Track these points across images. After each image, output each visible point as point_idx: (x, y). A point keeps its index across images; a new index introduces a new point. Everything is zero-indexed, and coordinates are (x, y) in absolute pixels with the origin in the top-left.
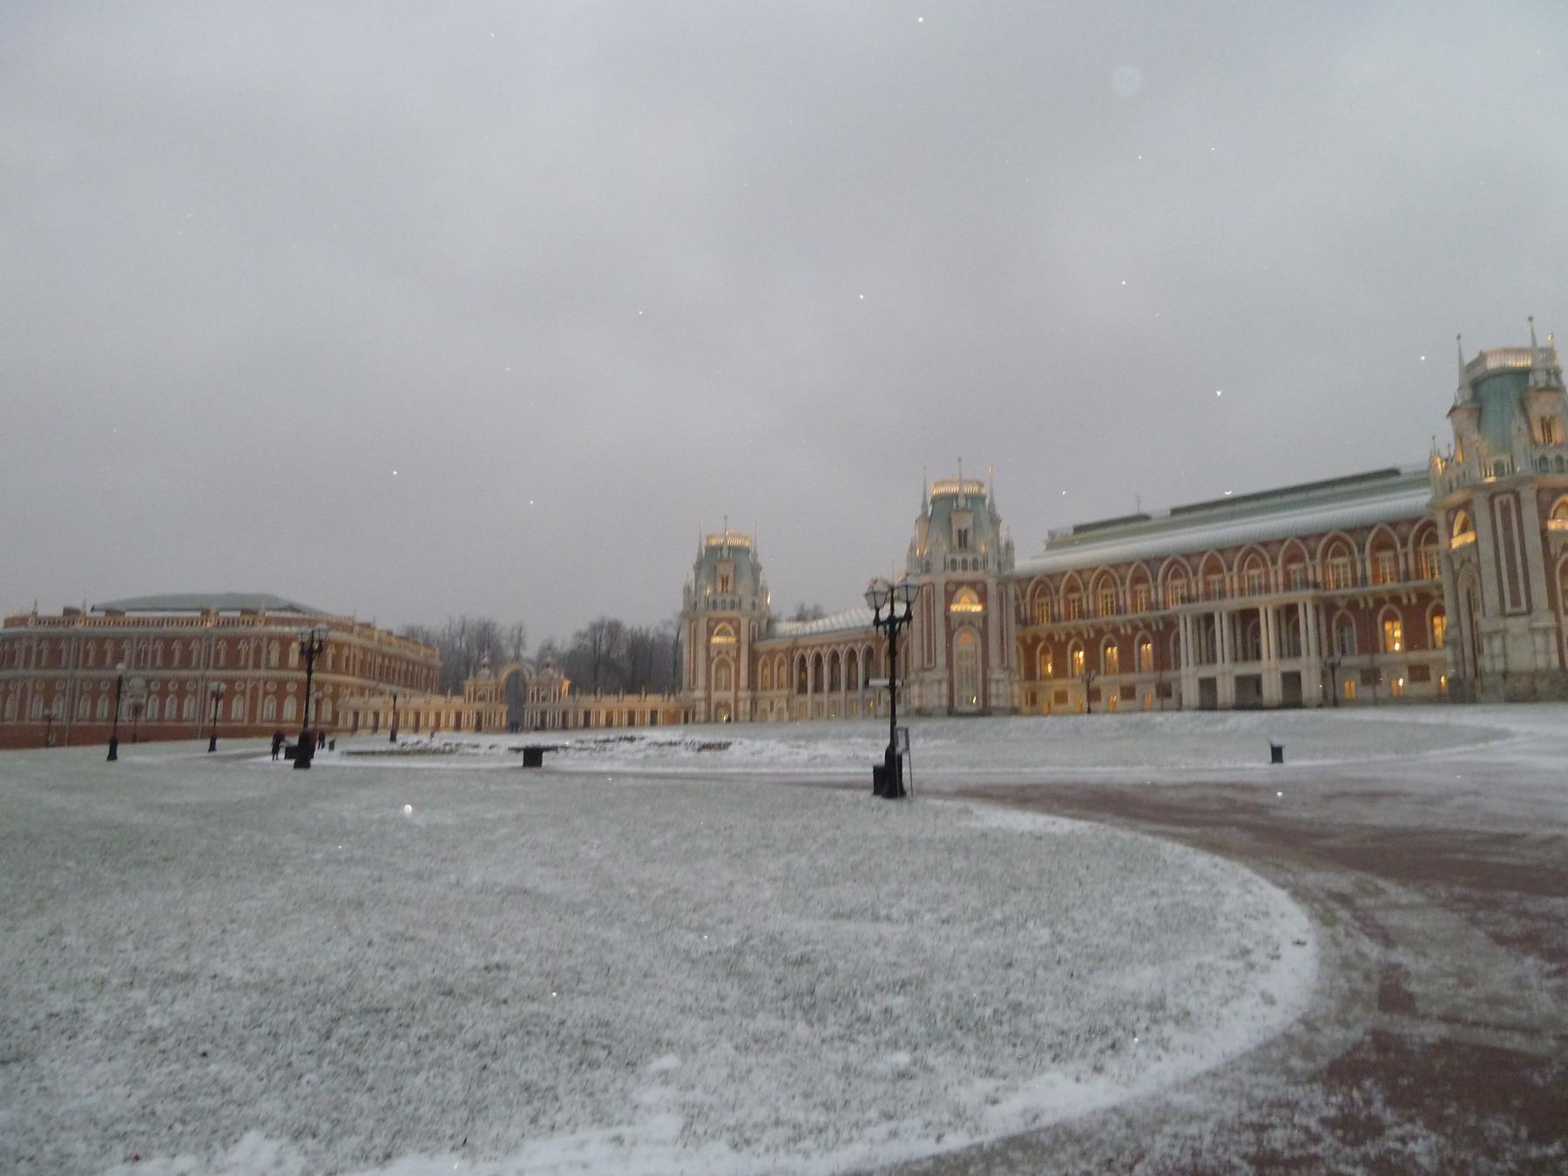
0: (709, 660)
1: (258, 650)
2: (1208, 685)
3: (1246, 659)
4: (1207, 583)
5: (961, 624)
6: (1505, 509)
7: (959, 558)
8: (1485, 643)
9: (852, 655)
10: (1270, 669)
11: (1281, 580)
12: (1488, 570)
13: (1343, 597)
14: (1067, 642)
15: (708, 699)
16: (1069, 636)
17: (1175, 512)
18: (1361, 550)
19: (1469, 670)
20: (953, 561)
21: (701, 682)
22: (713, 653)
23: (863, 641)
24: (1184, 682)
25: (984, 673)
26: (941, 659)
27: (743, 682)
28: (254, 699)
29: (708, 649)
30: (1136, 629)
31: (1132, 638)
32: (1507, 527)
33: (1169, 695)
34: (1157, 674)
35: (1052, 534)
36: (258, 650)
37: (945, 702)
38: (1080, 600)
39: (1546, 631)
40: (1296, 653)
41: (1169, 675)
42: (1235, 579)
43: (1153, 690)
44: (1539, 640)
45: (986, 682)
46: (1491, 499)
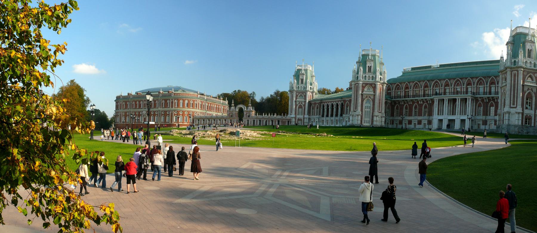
0: (296, 105)
2: (441, 121)
3: (453, 114)
4: (445, 90)
9: (337, 105)
10: (457, 118)
12: (508, 93)
13: (480, 98)
14: (403, 105)
16: (405, 103)
18: (487, 84)
19: (502, 123)
21: (294, 112)
22: (297, 103)
23: (341, 101)
25: (373, 114)
27: (306, 112)
30: (424, 102)
31: (422, 105)
35: (404, 70)
37: (359, 122)
39: (519, 113)
41: (431, 118)
43: (426, 123)
44: (517, 115)
45: (373, 117)
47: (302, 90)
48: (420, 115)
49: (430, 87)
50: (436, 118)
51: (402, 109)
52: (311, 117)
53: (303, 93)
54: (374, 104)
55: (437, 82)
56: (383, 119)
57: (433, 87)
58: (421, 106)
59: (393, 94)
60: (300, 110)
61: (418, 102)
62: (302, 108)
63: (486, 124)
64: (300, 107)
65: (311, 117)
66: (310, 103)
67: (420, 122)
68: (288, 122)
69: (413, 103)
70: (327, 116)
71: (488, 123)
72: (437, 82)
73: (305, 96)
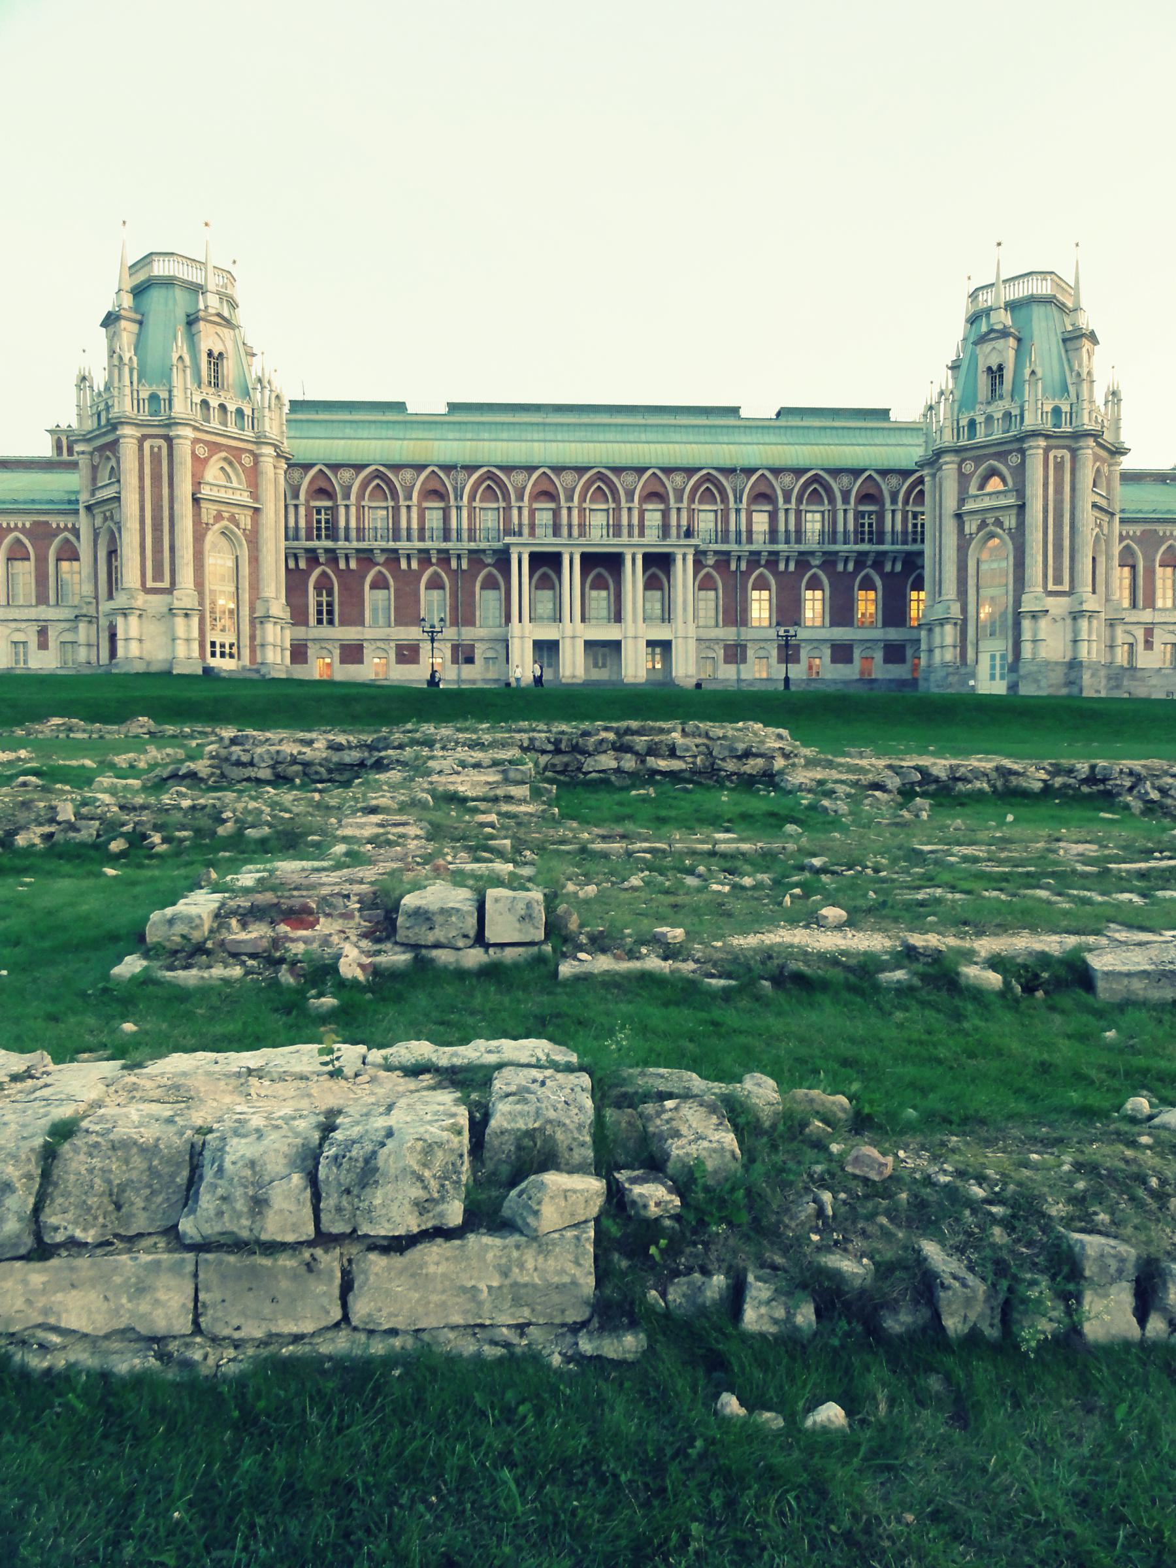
5: (219, 517)
6: (1059, 466)
7: (214, 403)
8: (1026, 624)
10: (635, 633)
11: (635, 521)
13: (716, 552)
14: (307, 574)
17: (454, 407)
18: (738, 499)
25: (252, 609)
32: (1059, 490)
33: (470, 660)
34: (454, 629)
38: (333, 510)
40: (667, 617)
42: (575, 513)
46: (1047, 450)
49: (459, 496)
54: (255, 560)
55: (490, 476)
56: (288, 634)
57: (472, 498)
63: (744, 660)
71: (750, 653)
72: (490, 476)
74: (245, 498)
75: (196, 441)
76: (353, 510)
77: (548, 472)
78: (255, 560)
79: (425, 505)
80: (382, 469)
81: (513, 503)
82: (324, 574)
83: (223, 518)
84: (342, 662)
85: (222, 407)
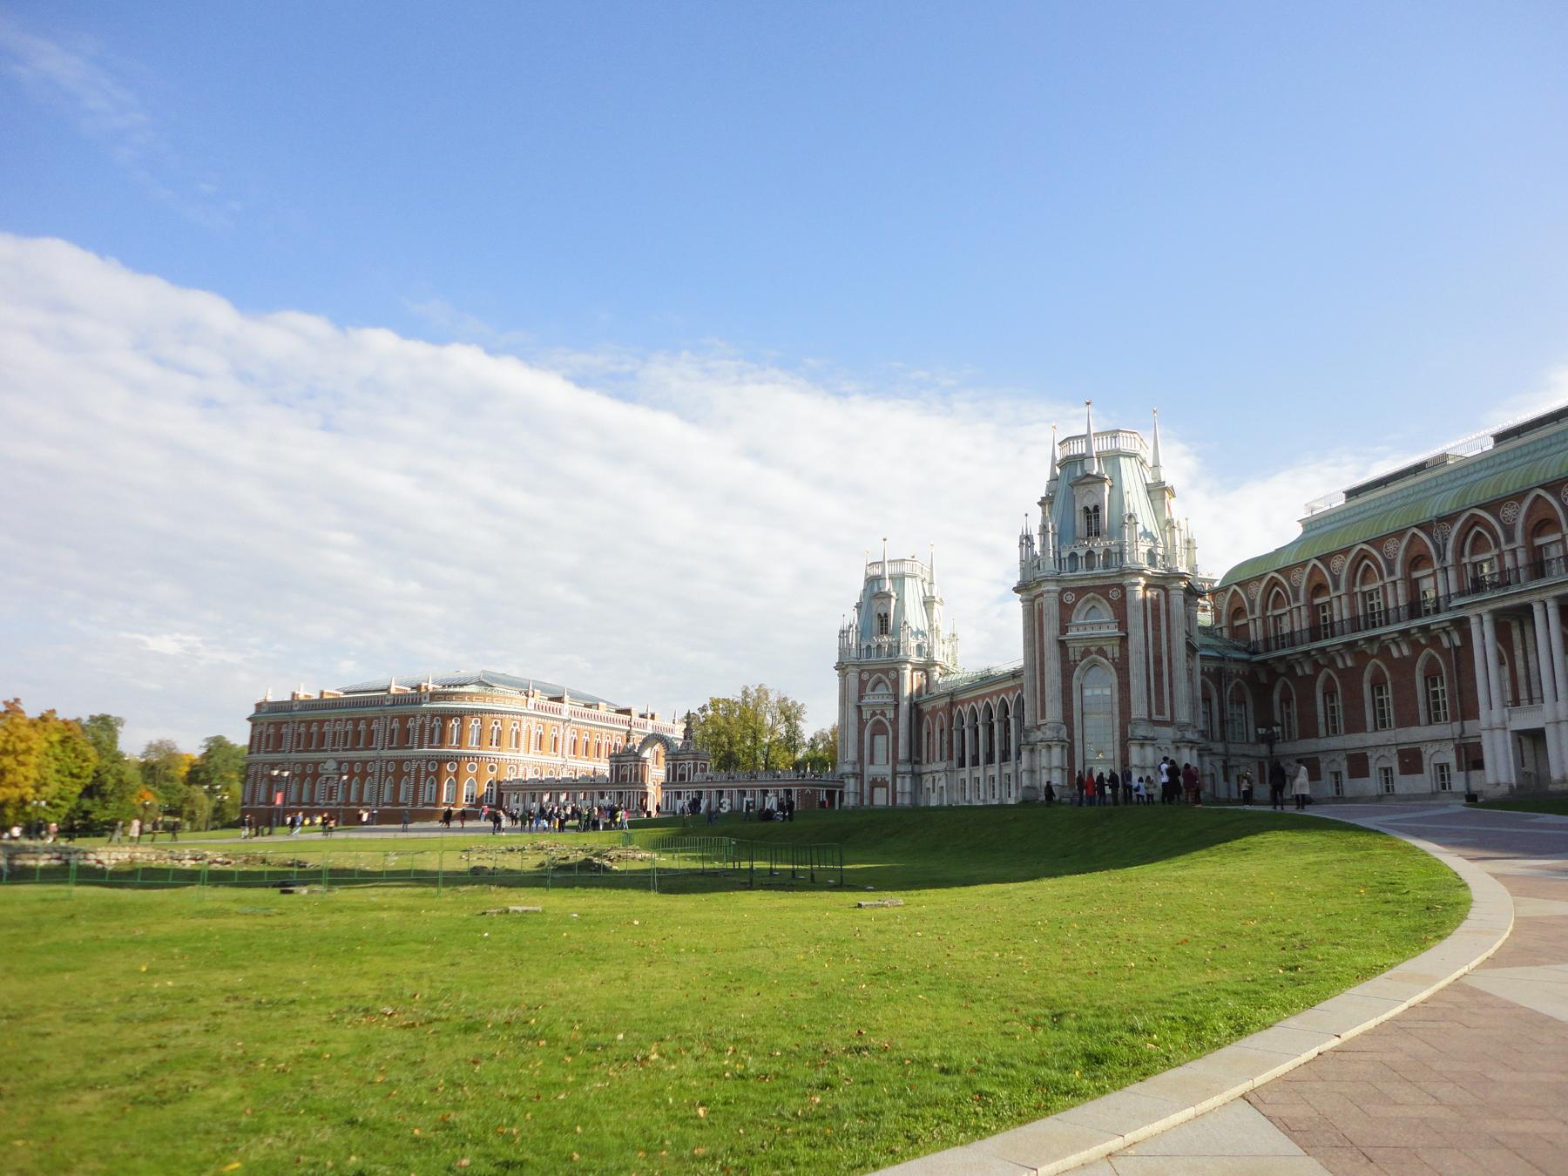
0: (861, 723)
1: (422, 726)
7: (1081, 553)
14: (1314, 678)
15: (859, 776)
16: (1317, 667)
20: (1073, 556)
22: (866, 715)
24: (1485, 735)
26: (1054, 712)
27: (903, 753)
28: (417, 779)
29: (859, 708)
31: (1410, 663)
34: (1457, 725)
36: (422, 726)
43: (1450, 758)
47: (884, 658)
48: (1408, 718)
50: (1495, 727)
51: (1307, 700)
52: (925, 769)
53: (886, 672)
54: (1124, 686)
57: (1460, 553)
58: (1403, 668)
59: (1256, 633)
60: (880, 741)
61: (1384, 652)
62: (885, 732)
64: (879, 729)
65: (925, 769)
66: (915, 708)
67: (1411, 760)
68: (830, 794)
69: (1362, 658)
70: (975, 762)
72: (1475, 521)
73: (897, 684)
74: (1113, 630)
75: (1064, 590)
76: (1345, 599)
77: (1542, 492)
78: (1124, 686)
79: (1416, 575)
80: (1365, 547)
81: (1504, 547)
82: (1329, 678)
83: (1090, 653)
84: (1351, 776)
85: (1090, 554)
